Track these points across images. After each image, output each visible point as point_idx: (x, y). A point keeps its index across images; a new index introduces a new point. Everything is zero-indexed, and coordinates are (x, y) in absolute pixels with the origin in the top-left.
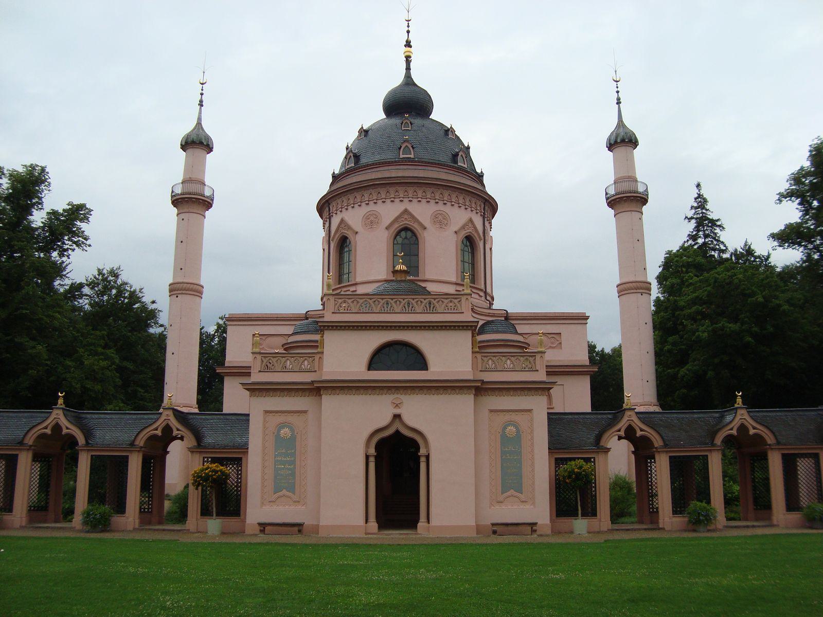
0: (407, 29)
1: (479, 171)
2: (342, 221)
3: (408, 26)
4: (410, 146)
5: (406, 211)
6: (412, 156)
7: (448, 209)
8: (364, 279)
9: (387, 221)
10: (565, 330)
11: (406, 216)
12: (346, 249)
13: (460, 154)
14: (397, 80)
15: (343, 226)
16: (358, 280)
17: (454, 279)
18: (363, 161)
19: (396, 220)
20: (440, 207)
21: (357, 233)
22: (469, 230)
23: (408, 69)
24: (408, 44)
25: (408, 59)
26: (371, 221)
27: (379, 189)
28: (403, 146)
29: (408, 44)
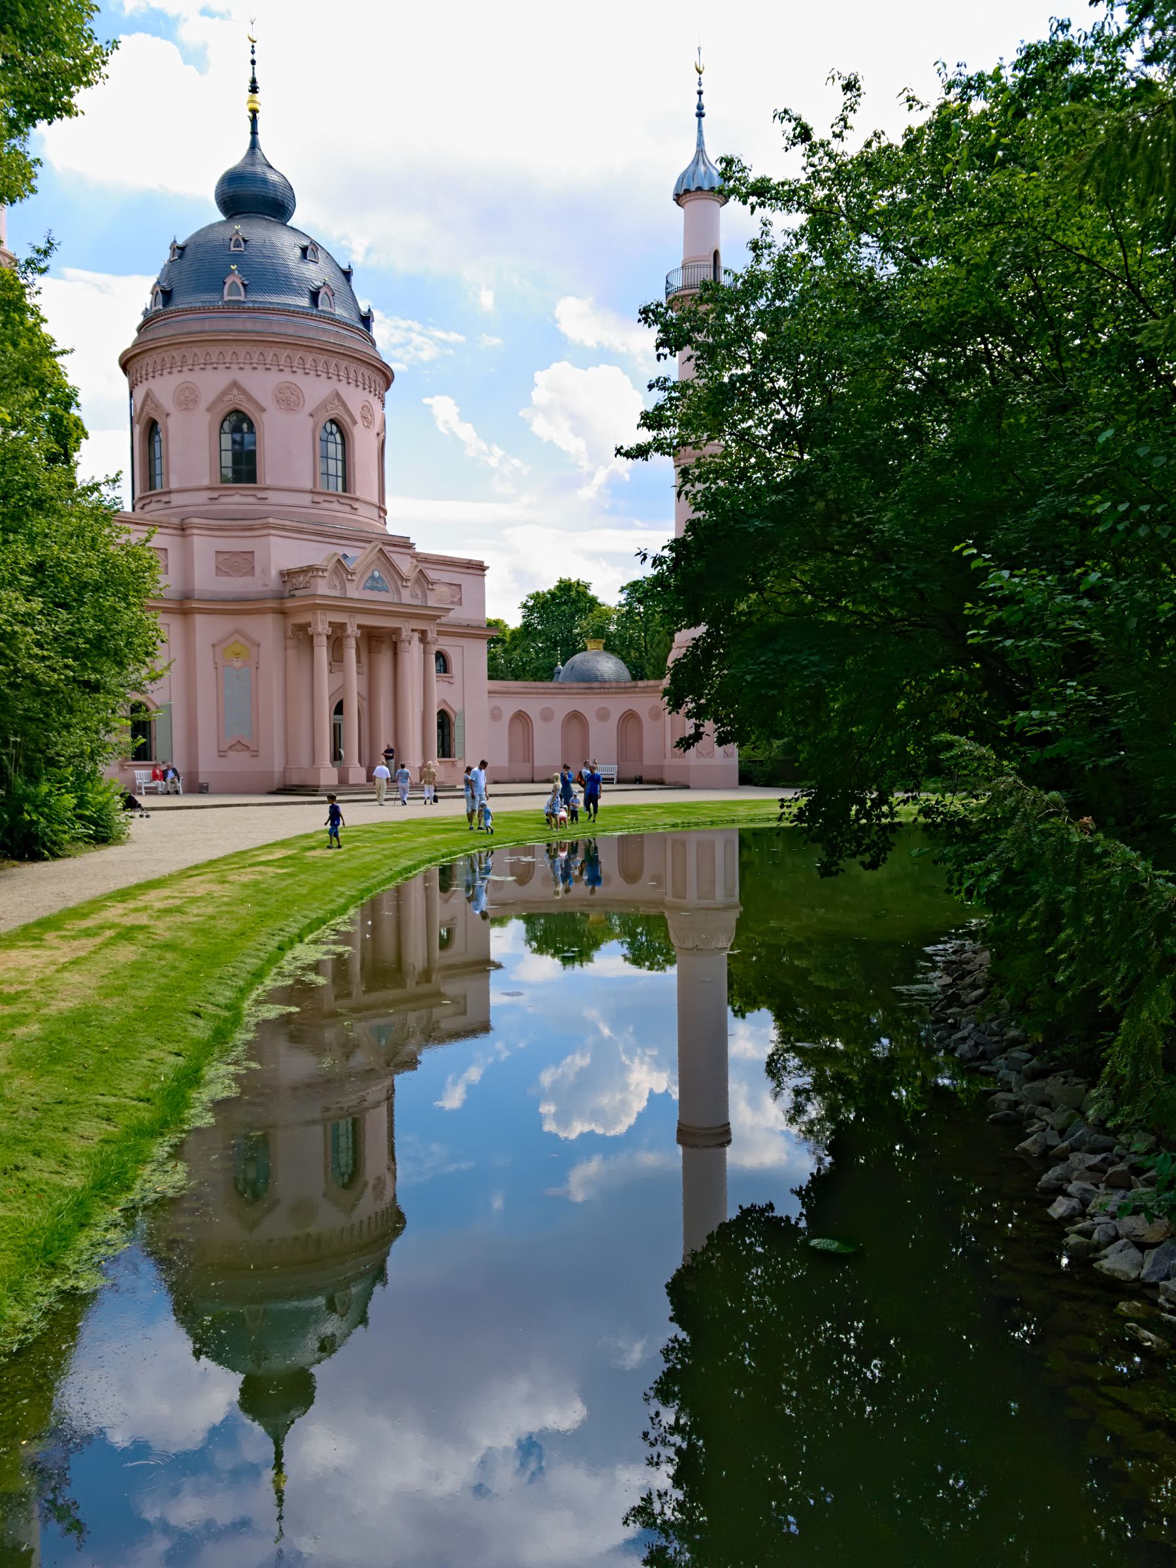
0: (251, 57)
2: (148, 396)
3: (253, 52)
4: (239, 282)
5: (235, 384)
7: (299, 379)
11: (235, 391)
12: (157, 438)
13: (322, 291)
14: (234, 156)
15: (149, 402)
16: (174, 484)
19: (220, 398)
20: (287, 377)
21: (168, 415)
22: (336, 412)
23: (254, 133)
24: (254, 89)
26: (187, 399)
27: (196, 350)
28: (229, 281)
29: (254, 89)
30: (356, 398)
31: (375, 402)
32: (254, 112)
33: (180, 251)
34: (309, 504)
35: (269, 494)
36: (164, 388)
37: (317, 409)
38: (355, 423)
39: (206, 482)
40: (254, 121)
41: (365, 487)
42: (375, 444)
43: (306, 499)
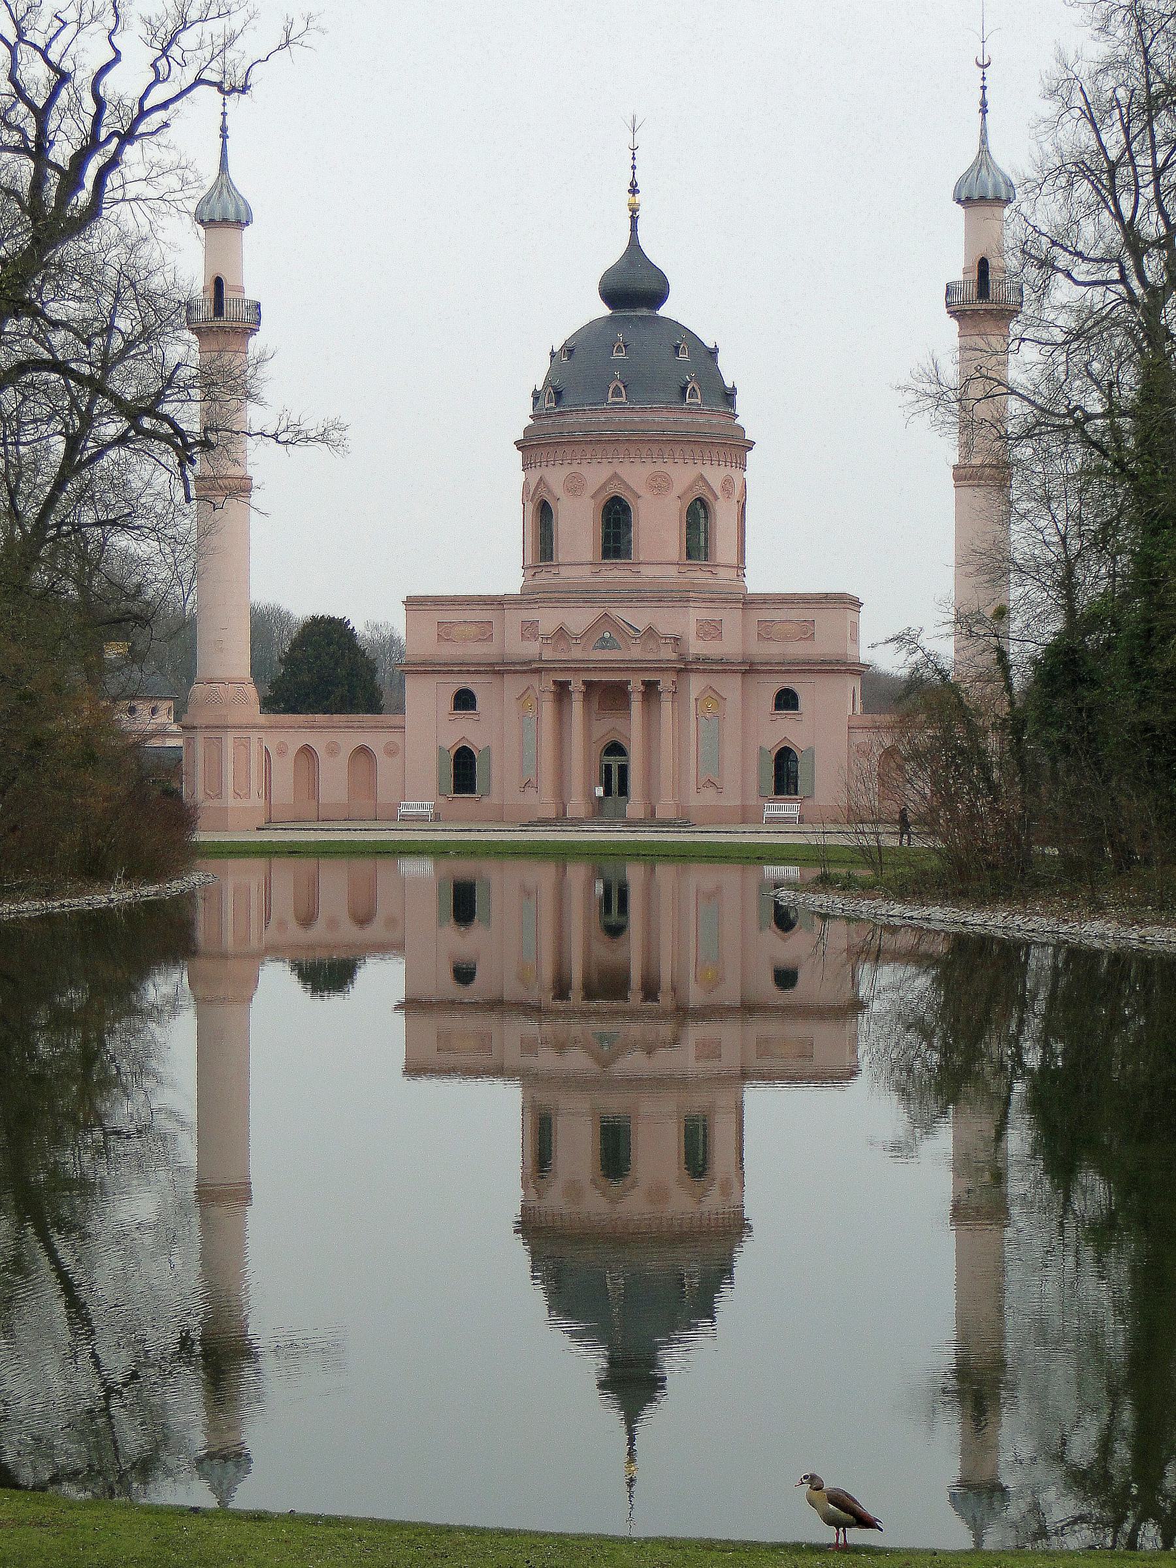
1: (729, 384)
3: (634, 158)
5: (615, 476)
6: (623, 399)
8: (568, 560)
9: (591, 489)
10: (823, 618)
11: (616, 482)
13: (690, 387)
17: (676, 559)
18: (568, 399)
19: (603, 487)
20: (660, 467)
23: (634, 229)
24: (634, 190)
25: (634, 220)
26: (575, 486)
29: (634, 190)
30: (715, 475)
31: (735, 473)
32: (634, 210)
33: (569, 350)
34: (676, 574)
35: (643, 569)
36: (556, 477)
37: (685, 493)
38: (716, 498)
39: (589, 557)
40: (634, 220)
41: (724, 550)
42: (735, 509)
43: (673, 571)
